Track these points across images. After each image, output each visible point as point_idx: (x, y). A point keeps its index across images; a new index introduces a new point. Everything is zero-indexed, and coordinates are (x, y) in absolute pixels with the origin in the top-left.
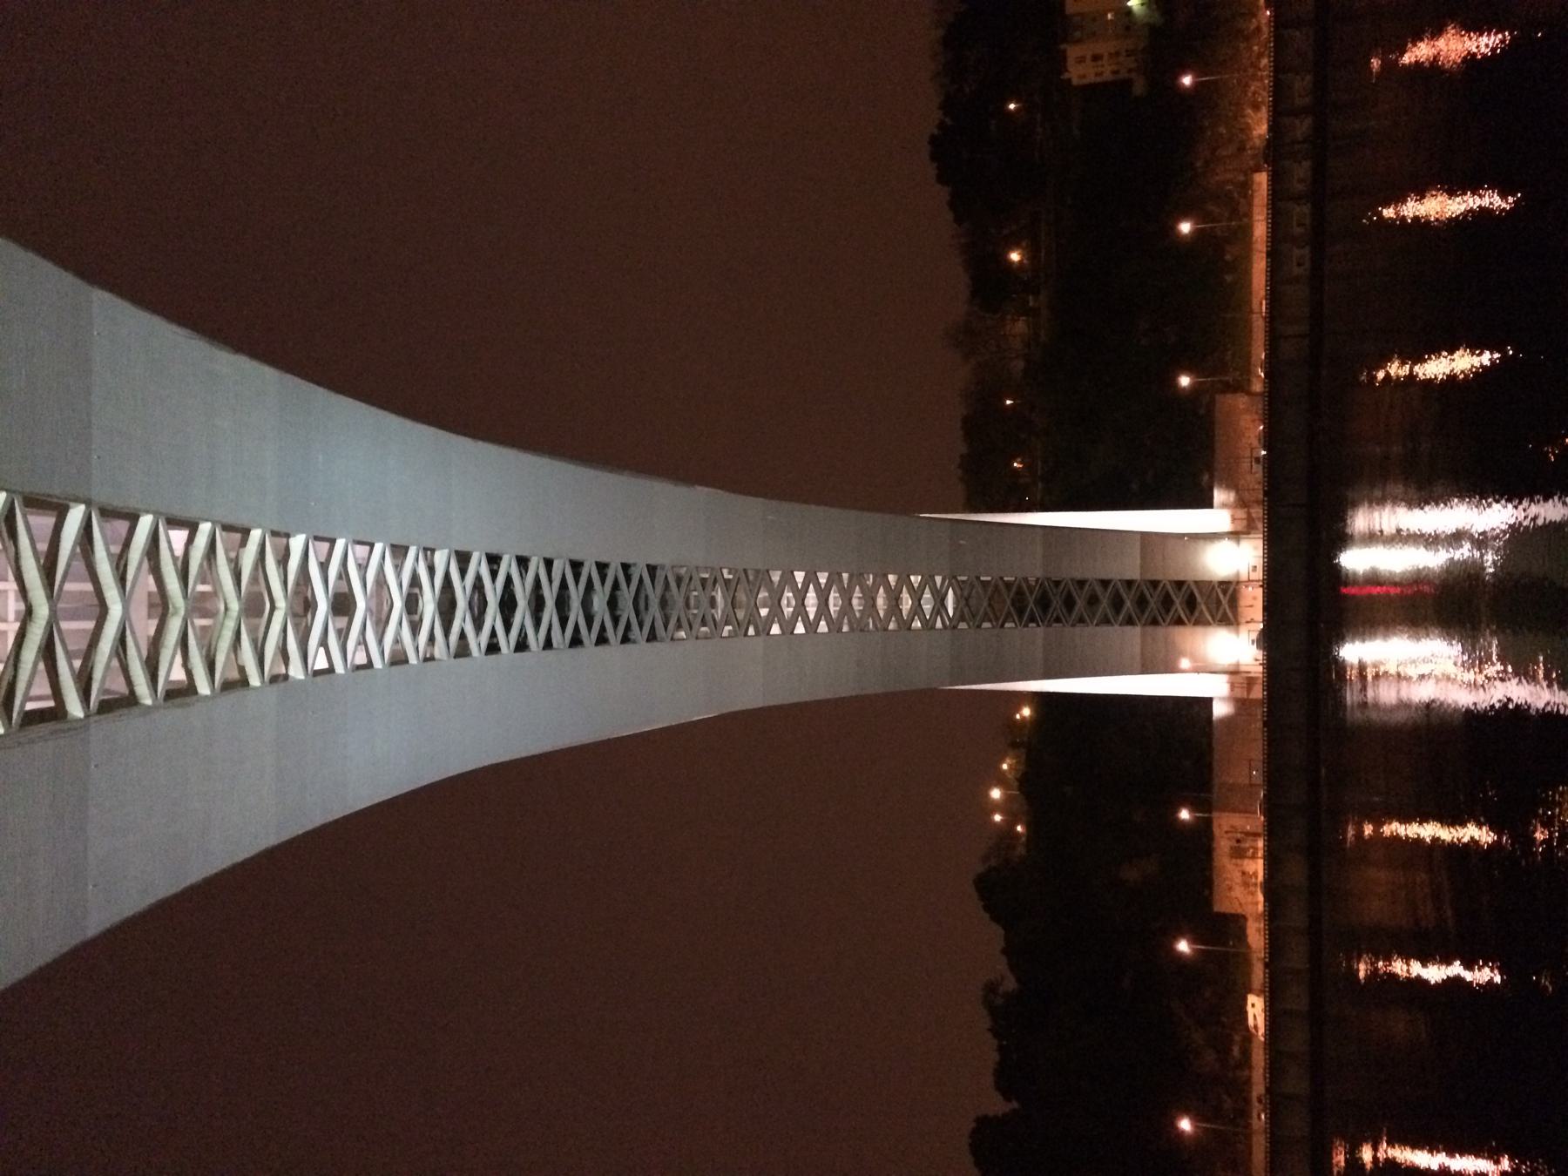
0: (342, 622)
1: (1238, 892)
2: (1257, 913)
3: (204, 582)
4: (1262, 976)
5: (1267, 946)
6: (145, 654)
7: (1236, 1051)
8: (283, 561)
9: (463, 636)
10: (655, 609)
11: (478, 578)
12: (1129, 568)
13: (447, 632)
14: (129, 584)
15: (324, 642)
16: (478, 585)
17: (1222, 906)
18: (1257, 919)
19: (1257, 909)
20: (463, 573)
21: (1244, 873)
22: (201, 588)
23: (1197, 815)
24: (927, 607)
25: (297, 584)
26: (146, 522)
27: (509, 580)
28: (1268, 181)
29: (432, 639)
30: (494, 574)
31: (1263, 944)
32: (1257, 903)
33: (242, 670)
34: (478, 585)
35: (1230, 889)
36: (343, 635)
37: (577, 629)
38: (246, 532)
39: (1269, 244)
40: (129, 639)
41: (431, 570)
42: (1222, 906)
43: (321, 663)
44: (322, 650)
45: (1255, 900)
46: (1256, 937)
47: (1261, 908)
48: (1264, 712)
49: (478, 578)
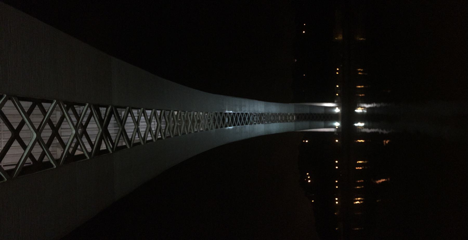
0: (199, 124)
3: (180, 119)
6: (172, 129)
8: (190, 116)
9: (217, 125)
10: (247, 119)
11: (219, 116)
12: (322, 111)
13: (214, 125)
14: (170, 120)
15: (196, 127)
16: (219, 118)
20: (216, 115)
22: (179, 120)
24: (291, 118)
25: (192, 119)
26: (172, 111)
27: (223, 117)
29: (212, 126)
30: (221, 115)
33: (185, 132)
34: (219, 118)
36: (199, 126)
37: (234, 123)
38: (185, 111)
40: (170, 128)
41: (212, 115)
43: (196, 130)
44: (196, 129)
49: (219, 116)
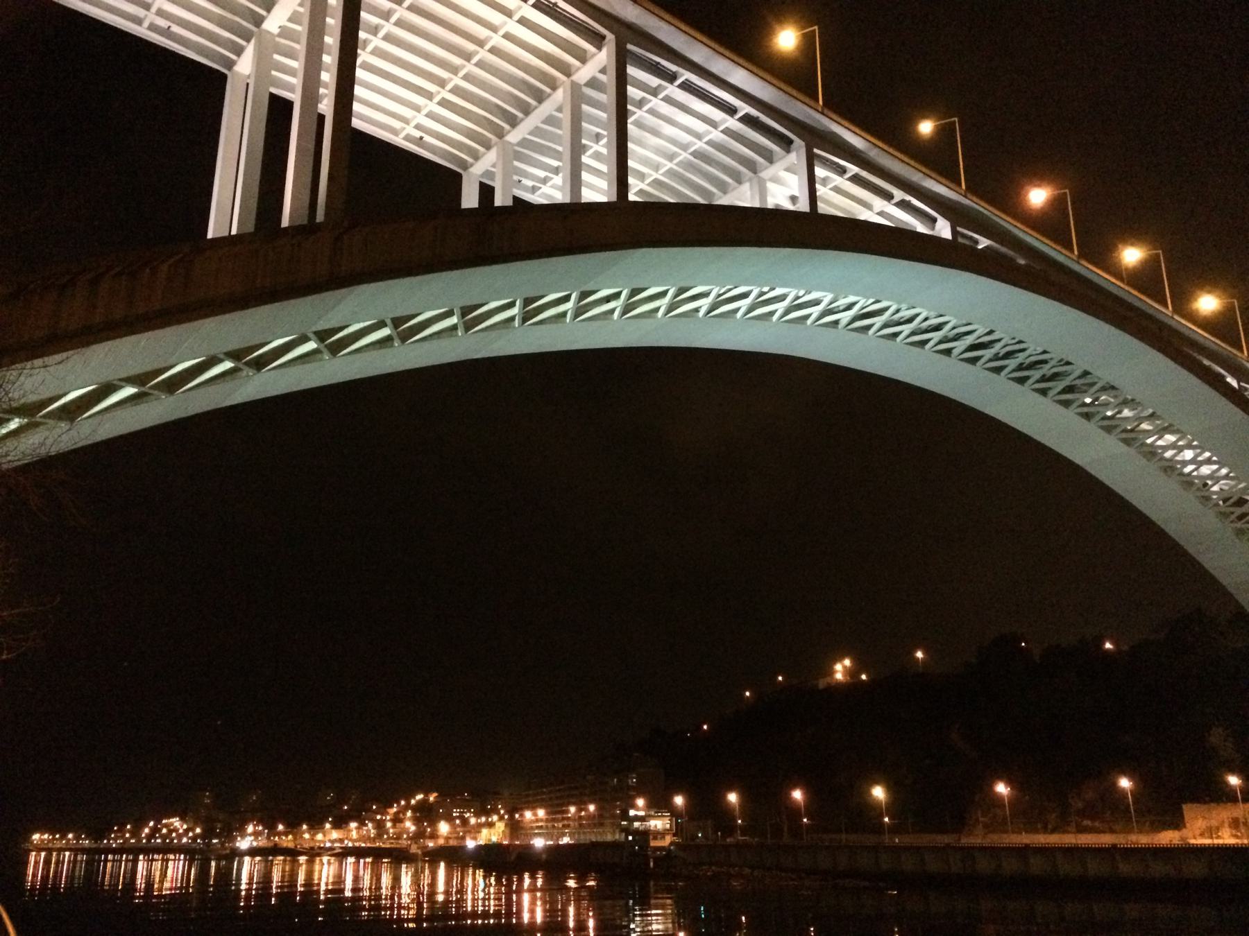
1: (1200, 824)
2: (1187, 838)
4: (1143, 842)
5: (1154, 846)
7: (1087, 823)
17: (1189, 810)
18: (1182, 839)
19: (1191, 839)
21: (1218, 829)
23: (1006, 798)
28: (1205, 844)
31: (1164, 843)
32: (1195, 838)
35: (1204, 818)
39: (1176, 846)
42: (1189, 810)
45: (1197, 837)
46: (1168, 838)
47: (1193, 841)
48: (1102, 844)
